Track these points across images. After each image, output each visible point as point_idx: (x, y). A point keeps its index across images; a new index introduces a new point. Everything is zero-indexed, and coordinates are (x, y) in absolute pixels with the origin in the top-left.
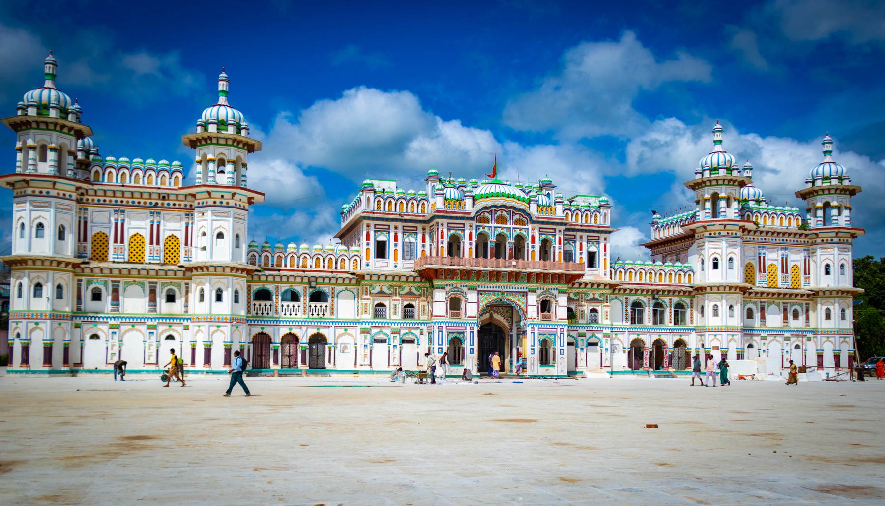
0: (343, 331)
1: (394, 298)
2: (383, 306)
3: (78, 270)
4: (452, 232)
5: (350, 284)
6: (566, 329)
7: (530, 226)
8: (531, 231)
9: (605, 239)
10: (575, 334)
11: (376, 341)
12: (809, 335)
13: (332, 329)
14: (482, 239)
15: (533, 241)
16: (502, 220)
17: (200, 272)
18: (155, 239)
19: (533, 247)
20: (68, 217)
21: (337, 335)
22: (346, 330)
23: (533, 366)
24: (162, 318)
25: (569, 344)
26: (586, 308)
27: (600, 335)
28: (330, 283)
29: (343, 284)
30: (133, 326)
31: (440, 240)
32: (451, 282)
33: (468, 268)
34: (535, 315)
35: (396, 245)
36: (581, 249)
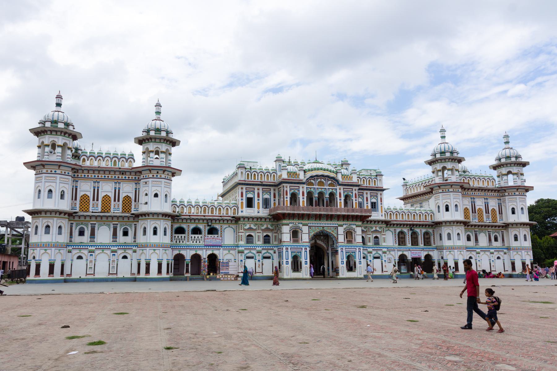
1: (258, 231)
3: (71, 218)
5: (231, 223)
6: (362, 248)
7: (338, 187)
8: (340, 191)
9: (381, 195)
10: (366, 252)
11: (248, 258)
12: (505, 251)
13: (221, 250)
14: (310, 196)
15: (340, 196)
16: (321, 184)
17: (144, 217)
18: (117, 198)
19: (340, 200)
20: (66, 186)
22: (229, 251)
23: (343, 272)
24: (120, 246)
25: (364, 258)
26: (372, 236)
27: (380, 252)
28: (219, 223)
29: (227, 223)
30: (103, 251)
31: (285, 196)
33: (302, 212)
35: (258, 200)
36: (367, 200)
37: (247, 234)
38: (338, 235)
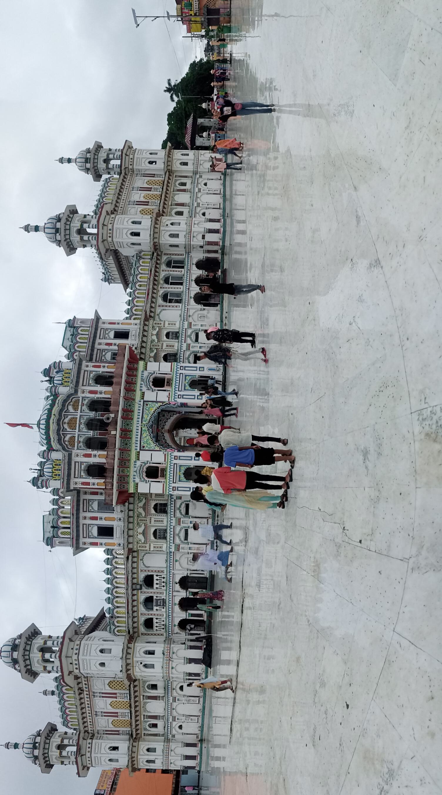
0: (177, 563)
1: (148, 522)
2: (156, 530)
4: (82, 474)
13: (175, 572)
21: (180, 568)
27: (189, 331)
32: (132, 477)
34: (166, 393)
37: (152, 538)
38: (157, 402)
